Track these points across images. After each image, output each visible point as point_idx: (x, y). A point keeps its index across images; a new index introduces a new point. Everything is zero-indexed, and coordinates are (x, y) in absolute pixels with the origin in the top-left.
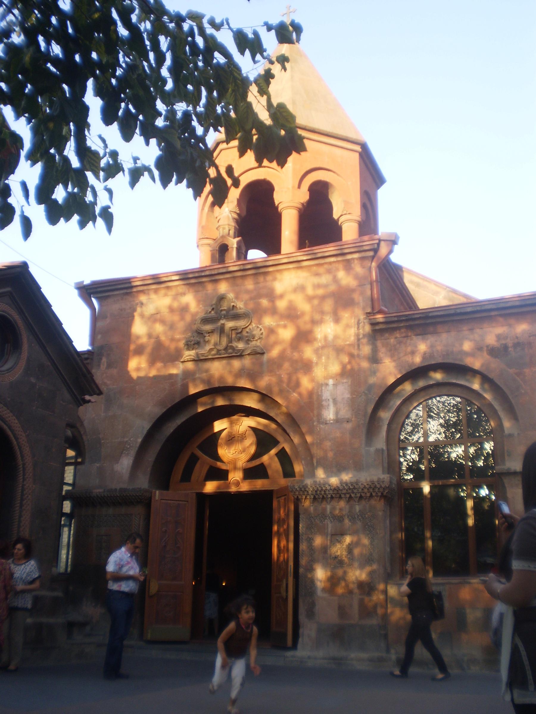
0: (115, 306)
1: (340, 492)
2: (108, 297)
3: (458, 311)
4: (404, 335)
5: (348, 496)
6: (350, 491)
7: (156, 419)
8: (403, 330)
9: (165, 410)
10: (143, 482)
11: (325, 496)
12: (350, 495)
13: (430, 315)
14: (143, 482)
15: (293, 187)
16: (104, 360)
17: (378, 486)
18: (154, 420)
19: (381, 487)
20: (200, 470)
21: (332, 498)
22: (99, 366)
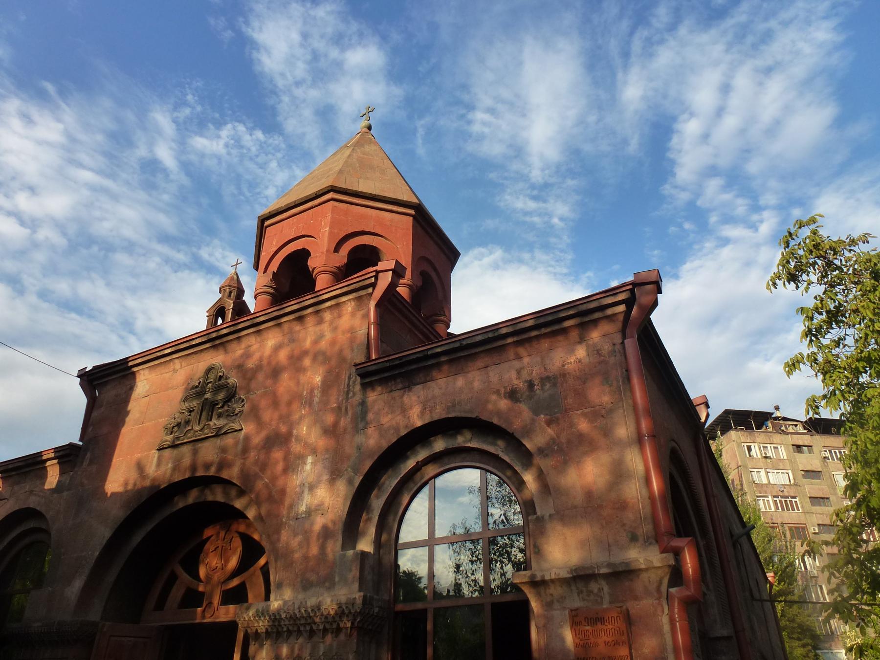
0: (109, 393)
1: (298, 622)
2: (106, 383)
3: (464, 343)
4: (400, 386)
5: (308, 628)
6: (309, 621)
7: (119, 523)
8: (398, 380)
9: (129, 512)
10: (95, 614)
11: (280, 629)
12: (311, 627)
13: (430, 353)
14: (95, 614)
15: (328, 251)
16: (88, 455)
17: (346, 612)
18: (116, 526)
19: (350, 612)
20: (177, 593)
21: (290, 632)
22: (82, 462)
